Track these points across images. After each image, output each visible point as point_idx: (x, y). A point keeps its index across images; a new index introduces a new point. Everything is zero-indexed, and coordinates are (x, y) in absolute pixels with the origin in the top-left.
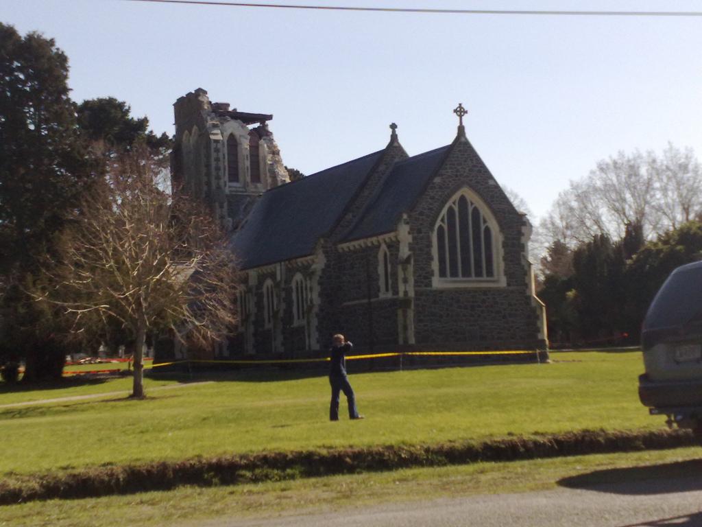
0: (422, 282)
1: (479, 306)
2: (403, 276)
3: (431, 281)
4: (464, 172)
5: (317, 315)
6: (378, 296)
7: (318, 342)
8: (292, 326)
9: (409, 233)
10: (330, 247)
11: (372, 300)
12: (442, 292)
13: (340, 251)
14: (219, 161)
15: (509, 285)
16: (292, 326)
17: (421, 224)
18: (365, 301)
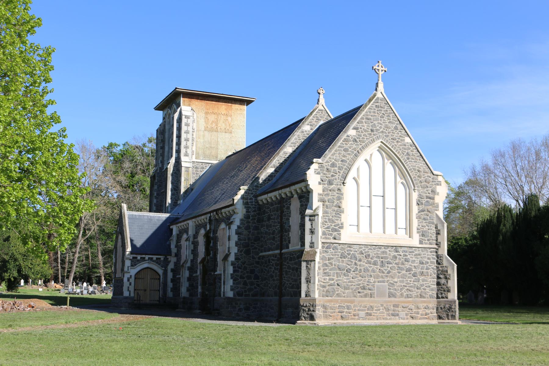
0: (331, 235)
1: (389, 263)
2: (310, 227)
3: (340, 234)
4: (381, 128)
5: (233, 264)
6: (288, 248)
7: (231, 290)
8: (216, 273)
9: (320, 183)
10: (251, 199)
11: (283, 251)
12: (350, 245)
13: (261, 203)
14: (188, 133)
15: (421, 242)
16: (216, 273)
17: (332, 176)
18: (277, 252)
